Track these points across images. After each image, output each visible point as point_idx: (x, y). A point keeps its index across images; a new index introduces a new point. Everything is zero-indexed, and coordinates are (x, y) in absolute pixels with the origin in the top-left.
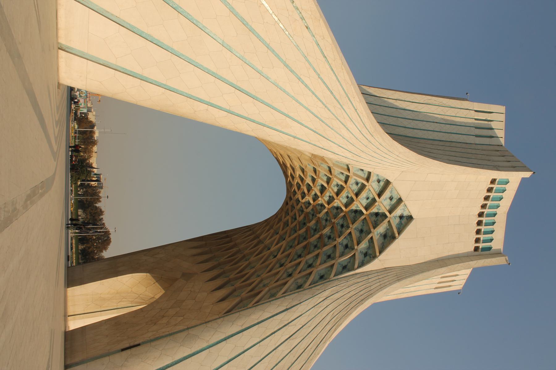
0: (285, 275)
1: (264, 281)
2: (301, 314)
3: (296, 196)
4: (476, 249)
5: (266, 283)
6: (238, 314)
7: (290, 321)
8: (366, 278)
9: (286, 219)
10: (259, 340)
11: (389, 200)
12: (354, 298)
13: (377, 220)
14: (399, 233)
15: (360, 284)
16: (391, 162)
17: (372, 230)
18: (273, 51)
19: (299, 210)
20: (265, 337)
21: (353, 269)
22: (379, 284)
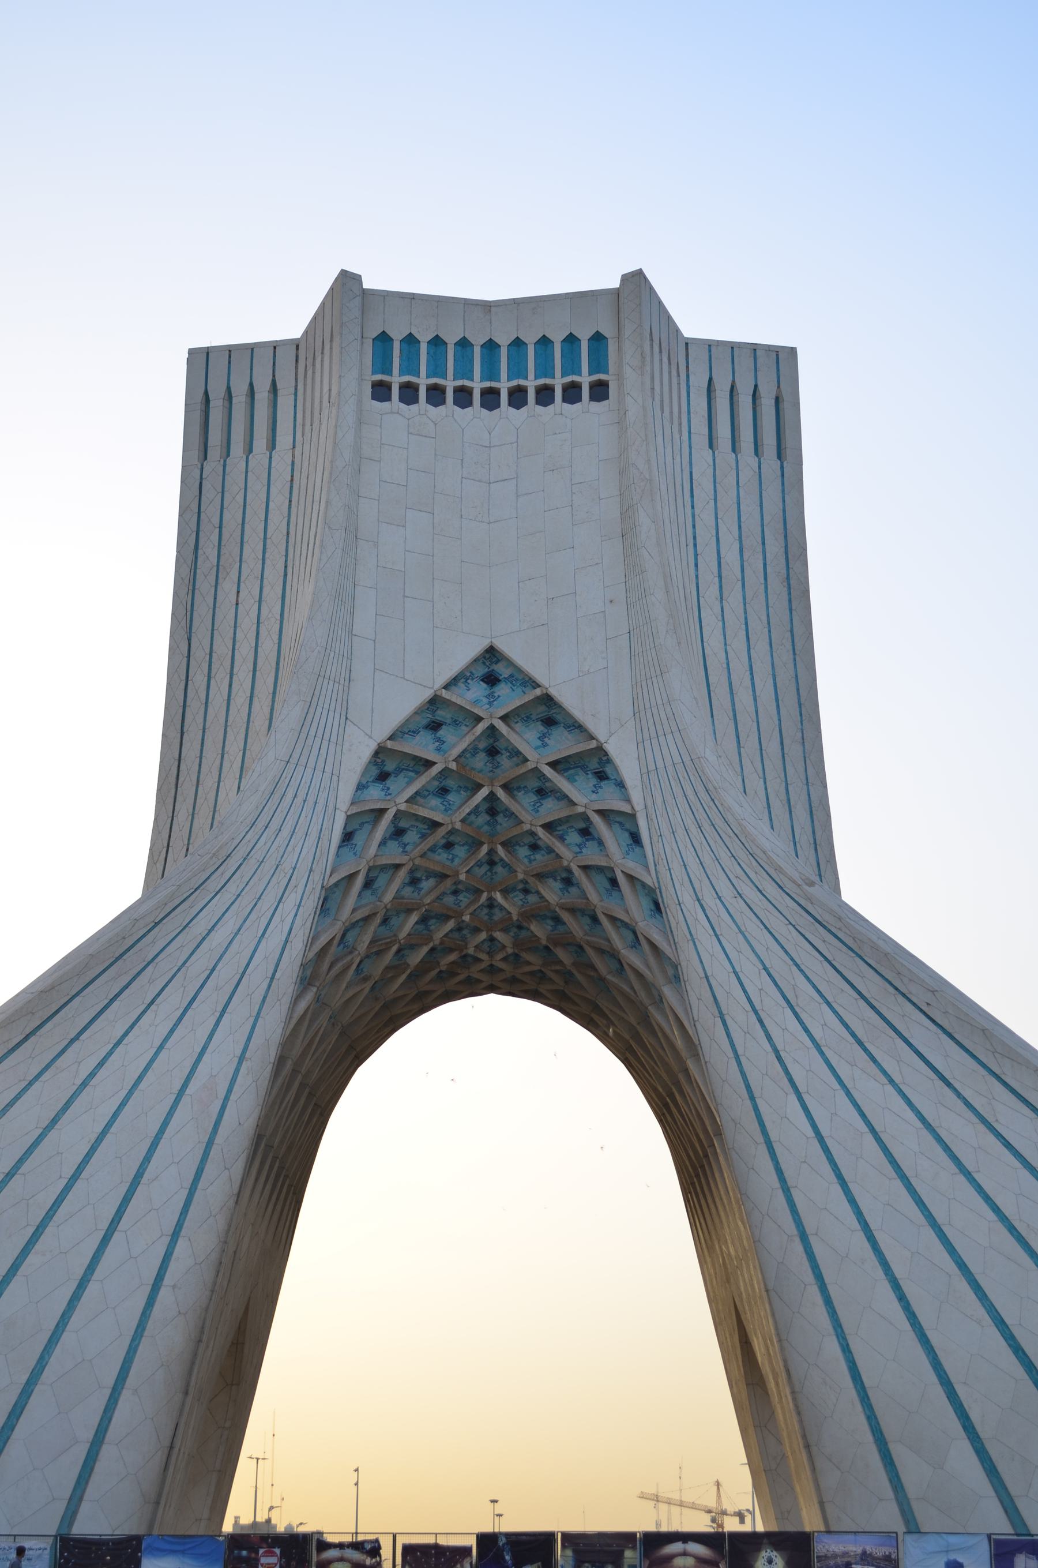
2: (733, 975)
4: (600, 391)
7: (748, 1008)
8: (653, 775)
10: (793, 1098)
11: (441, 733)
12: (701, 815)
13: (506, 749)
14: (536, 685)
16: (309, 771)
17: (530, 765)
18: (21, 1161)
21: (632, 816)
22: (669, 737)
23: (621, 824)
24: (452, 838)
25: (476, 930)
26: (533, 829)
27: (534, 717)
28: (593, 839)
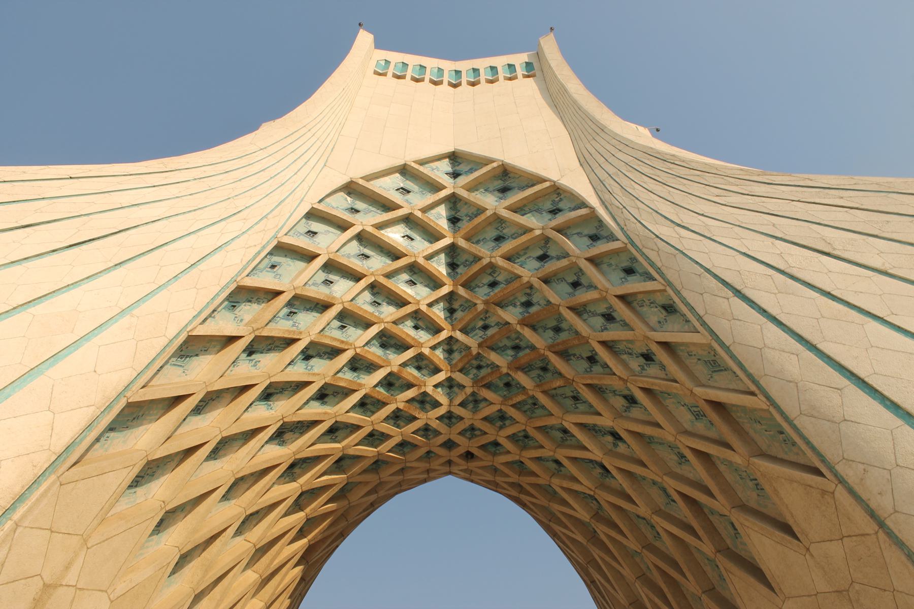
0: (653, 370)
1: (687, 426)
3: (435, 424)
5: (689, 416)
6: (806, 425)
8: (609, 182)
9: (507, 445)
12: (663, 177)
13: (467, 215)
15: (625, 182)
17: (488, 213)
19: (475, 410)
20: (853, 313)
23: (578, 234)
26: (493, 260)
27: (491, 189)
28: (552, 258)
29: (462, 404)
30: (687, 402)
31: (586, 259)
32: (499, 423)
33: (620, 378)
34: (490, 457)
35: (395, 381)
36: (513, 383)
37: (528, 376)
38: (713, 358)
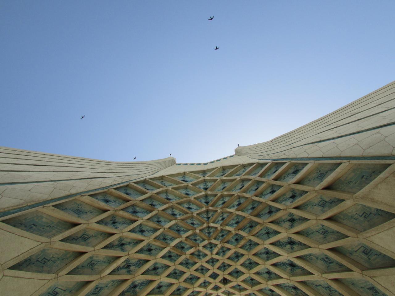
23: (254, 174)
24: (190, 206)
25: (204, 240)
29: (217, 254)
30: (316, 202)
31: (258, 177)
32: (236, 260)
33: (283, 209)
34: (235, 280)
35: (185, 246)
36: (239, 238)
37: (245, 232)
38: (320, 173)
